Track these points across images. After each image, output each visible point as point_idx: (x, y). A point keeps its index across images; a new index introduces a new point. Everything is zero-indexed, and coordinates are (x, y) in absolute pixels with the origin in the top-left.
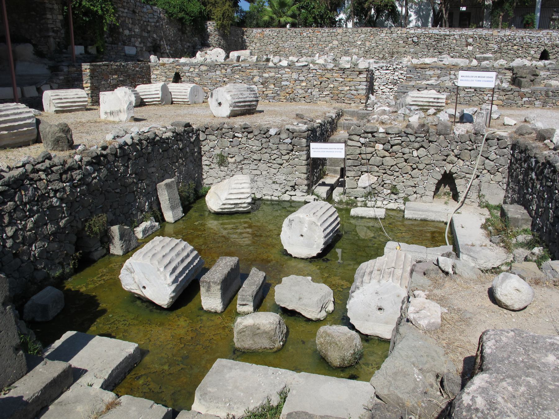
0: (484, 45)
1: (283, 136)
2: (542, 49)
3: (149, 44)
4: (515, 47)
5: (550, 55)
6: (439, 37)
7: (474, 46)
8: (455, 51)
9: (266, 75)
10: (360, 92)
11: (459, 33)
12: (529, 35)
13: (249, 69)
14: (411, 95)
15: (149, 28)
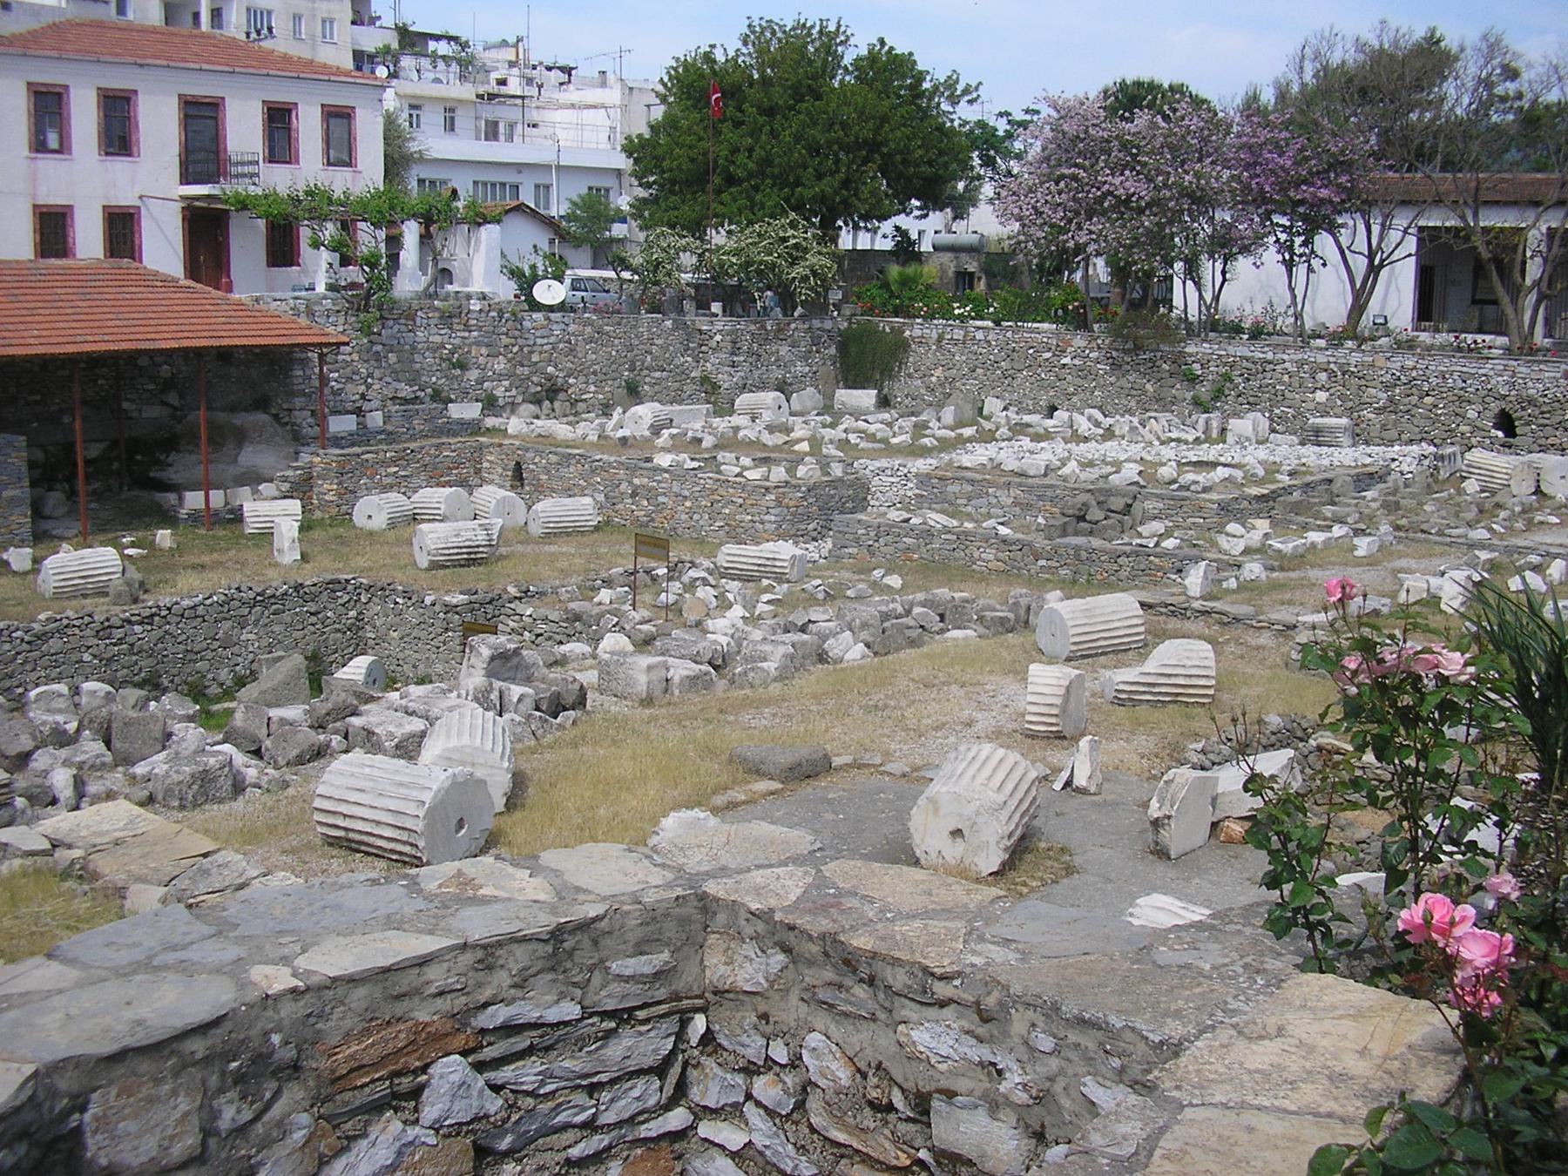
0: (1354, 389)
1: (437, 608)
2: (1495, 407)
3: (534, 389)
4: (1428, 400)
5: (1516, 423)
6: (1250, 365)
7: (1332, 391)
8: (1286, 403)
9: (636, 481)
10: (768, 526)
11: (1296, 357)
12: (1459, 368)
13: (614, 468)
14: (726, 551)
15: (535, 358)
